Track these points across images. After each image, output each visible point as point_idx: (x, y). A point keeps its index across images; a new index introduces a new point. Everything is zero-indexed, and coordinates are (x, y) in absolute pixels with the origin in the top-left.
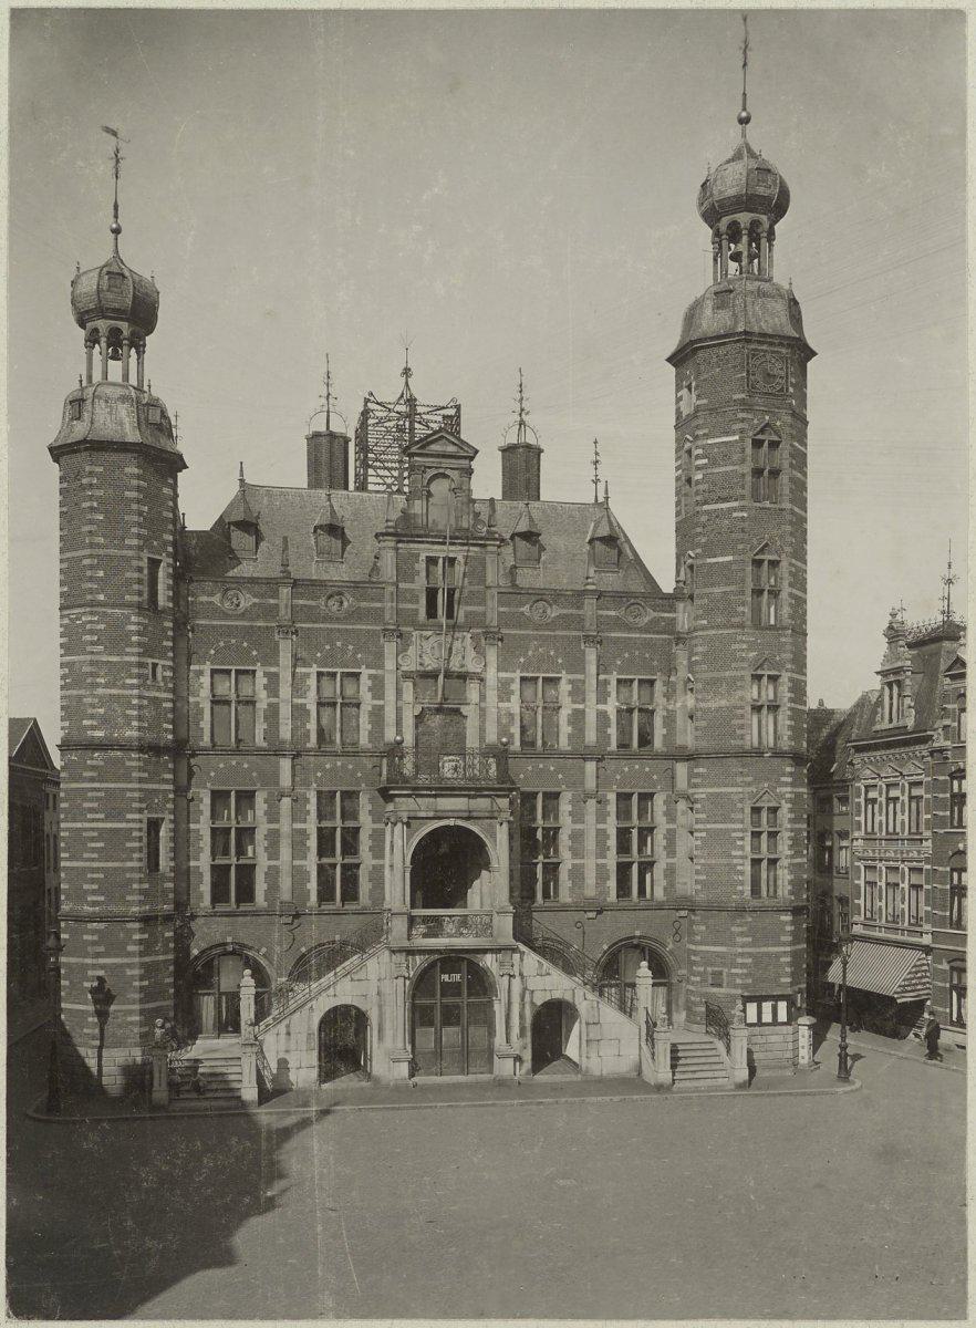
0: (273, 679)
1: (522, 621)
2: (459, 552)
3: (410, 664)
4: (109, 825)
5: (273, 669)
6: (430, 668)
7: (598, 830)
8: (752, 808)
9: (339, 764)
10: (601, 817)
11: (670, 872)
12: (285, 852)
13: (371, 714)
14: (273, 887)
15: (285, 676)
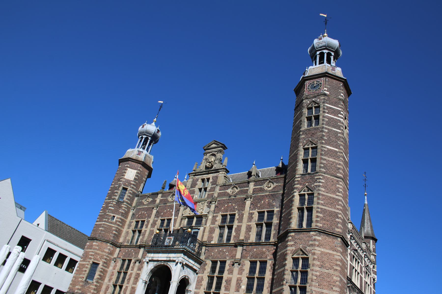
0: (148, 222)
8: (293, 259)
10: (241, 271)
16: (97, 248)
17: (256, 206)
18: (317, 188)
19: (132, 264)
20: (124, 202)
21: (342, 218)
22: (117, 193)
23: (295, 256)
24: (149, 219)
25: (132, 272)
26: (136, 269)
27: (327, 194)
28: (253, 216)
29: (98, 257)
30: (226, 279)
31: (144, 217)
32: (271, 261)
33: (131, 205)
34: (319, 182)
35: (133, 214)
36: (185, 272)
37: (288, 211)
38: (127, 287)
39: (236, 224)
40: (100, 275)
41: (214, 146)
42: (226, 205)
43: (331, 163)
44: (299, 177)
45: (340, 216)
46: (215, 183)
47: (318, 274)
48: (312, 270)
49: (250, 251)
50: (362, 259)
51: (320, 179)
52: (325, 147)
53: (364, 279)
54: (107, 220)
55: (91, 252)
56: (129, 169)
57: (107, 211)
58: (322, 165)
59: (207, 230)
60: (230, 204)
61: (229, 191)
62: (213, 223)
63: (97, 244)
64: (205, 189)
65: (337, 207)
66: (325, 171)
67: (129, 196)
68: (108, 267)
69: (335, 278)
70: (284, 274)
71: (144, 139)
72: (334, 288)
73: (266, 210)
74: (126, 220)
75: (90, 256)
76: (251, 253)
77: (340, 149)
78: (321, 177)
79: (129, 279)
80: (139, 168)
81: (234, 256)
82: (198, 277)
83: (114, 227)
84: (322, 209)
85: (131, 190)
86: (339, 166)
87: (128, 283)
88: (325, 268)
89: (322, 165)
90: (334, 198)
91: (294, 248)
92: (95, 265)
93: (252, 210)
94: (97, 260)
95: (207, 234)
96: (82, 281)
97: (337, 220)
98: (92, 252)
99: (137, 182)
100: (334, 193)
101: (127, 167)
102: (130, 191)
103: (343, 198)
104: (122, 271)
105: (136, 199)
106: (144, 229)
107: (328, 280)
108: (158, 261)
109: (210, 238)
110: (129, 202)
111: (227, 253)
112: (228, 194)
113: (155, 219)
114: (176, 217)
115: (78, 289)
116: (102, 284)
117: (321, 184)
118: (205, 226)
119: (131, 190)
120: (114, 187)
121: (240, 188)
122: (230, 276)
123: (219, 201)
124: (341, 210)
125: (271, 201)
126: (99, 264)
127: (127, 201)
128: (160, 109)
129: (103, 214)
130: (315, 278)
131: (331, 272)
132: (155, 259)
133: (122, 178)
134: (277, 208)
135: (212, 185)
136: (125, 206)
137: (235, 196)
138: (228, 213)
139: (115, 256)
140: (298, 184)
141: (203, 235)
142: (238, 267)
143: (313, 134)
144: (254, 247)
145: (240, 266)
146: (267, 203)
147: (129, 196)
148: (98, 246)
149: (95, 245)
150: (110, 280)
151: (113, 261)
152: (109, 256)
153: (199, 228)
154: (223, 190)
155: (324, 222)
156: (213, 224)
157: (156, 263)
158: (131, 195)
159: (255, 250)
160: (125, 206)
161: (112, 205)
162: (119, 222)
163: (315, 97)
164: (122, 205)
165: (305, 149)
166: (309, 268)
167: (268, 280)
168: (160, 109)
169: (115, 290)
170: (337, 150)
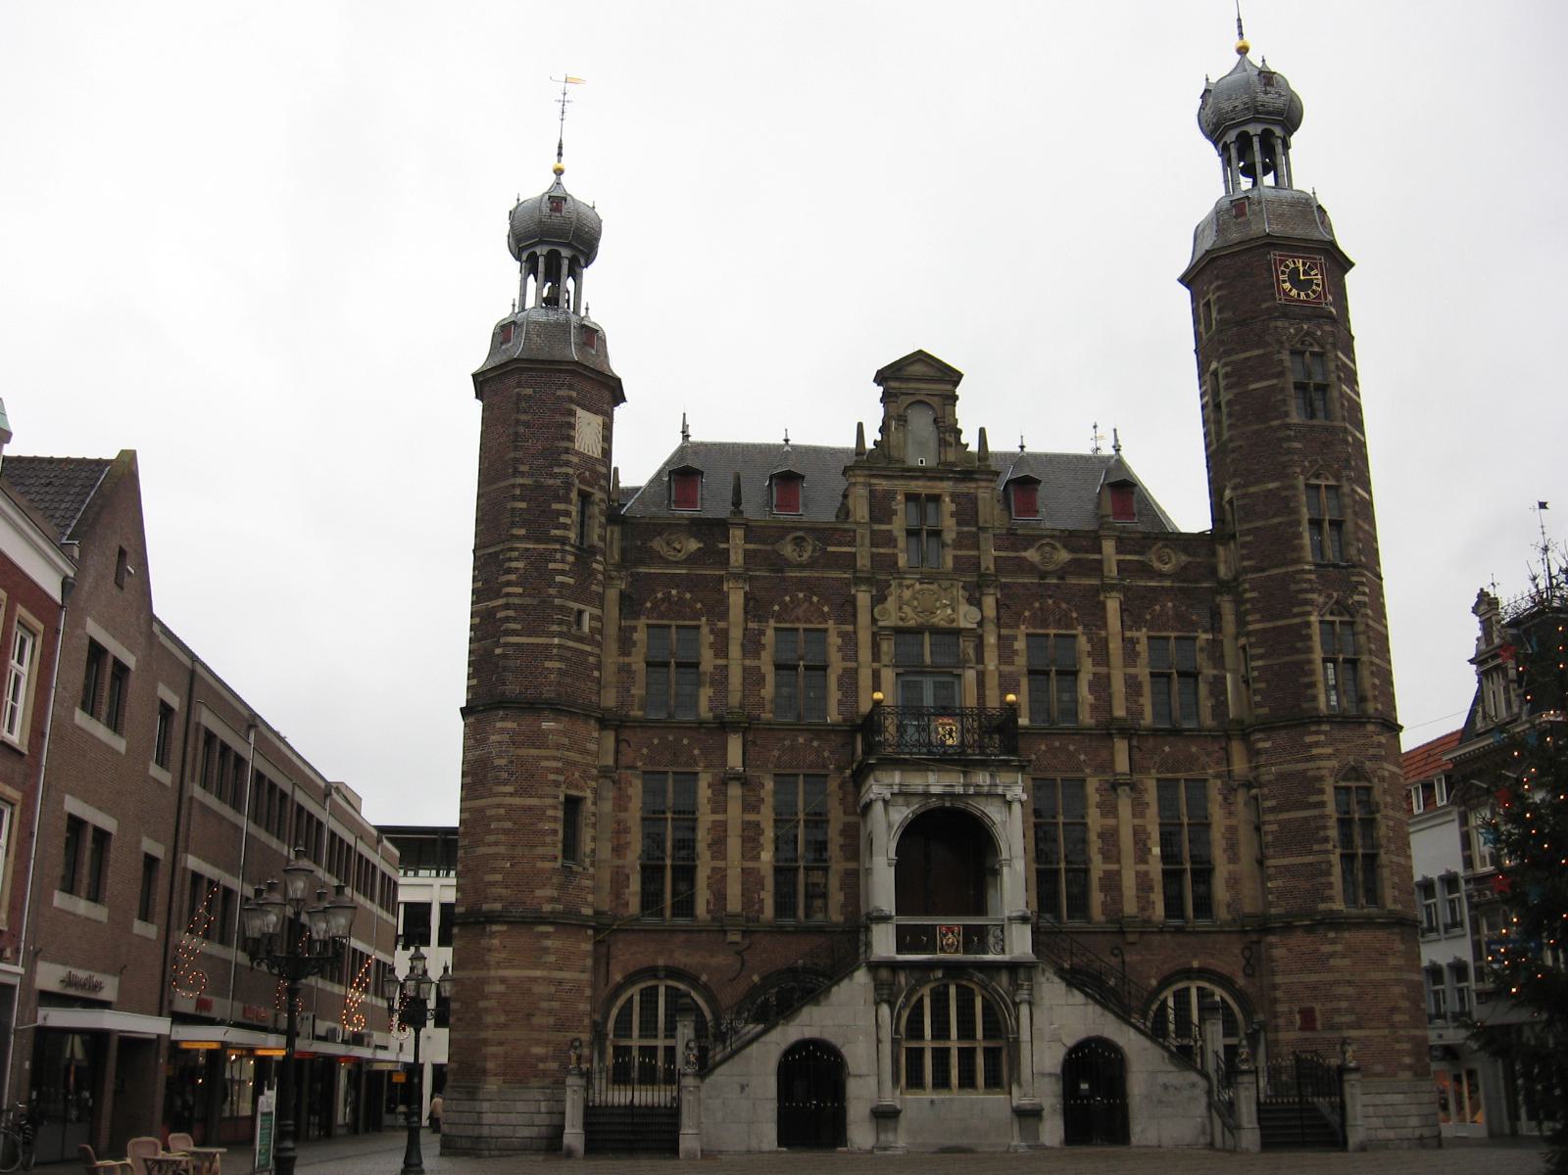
2: (945, 487)
3: (890, 616)
4: (517, 801)
5: (721, 625)
6: (912, 623)
8: (1336, 788)
9: (801, 740)
11: (1233, 882)
12: (734, 845)
13: (840, 679)
14: (720, 897)
15: (736, 634)
16: (566, 741)
18: (1363, 610)
19: (704, 792)
20: (592, 551)
23: (1343, 784)
24: (721, 625)
26: (734, 810)
28: (1138, 648)
29: (577, 774)
30: (1099, 830)
32: (1219, 782)
34: (1364, 594)
35: (624, 597)
39: (1087, 671)
41: (918, 369)
42: (1037, 605)
44: (1310, 572)
48: (1386, 817)
51: (1362, 584)
56: (580, 412)
57: (552, 591)
61: (1031, 555)
63: (561, 727)
64: (936, 533)
70: (1325, 828)
73: (1173, 634)
75: (552, 777)
76: (1157, 758)
81: (1108, 766)
91: (1334, 763)
92: (572, 804)
93: (1131, 629)
94: (577, 787)
98: (555, 759)
101: (571, 400)
106: (708, 661)
108: (927, 795)
111: (1082, 757)
112: (1031, 568)
113: (751, 625)
118: (980, 667)
121: (1072, 550)
122: (1111, 822)
123: (1003, 587)
125: (1183, 608)
129: (528, 601)
132: (912, 789)
133: (567, 451)
134: (1205, 631)
135: (958, 524)
136: (600, 568)
138: (1052, 632)
140: (1312, 591)
142: (1128, 797)
143: (1324, 443)
145: (1133, 795)
148: (565, 733)
150: (618, 850)
153: (956, 671)
154: (1007, 549)
156: (1005, 663)
160: (600, 568)
161: (567, 568)
163: (1308, 318)
164: (595, 565)
166: (1378, 812)
167: (1223, 830)
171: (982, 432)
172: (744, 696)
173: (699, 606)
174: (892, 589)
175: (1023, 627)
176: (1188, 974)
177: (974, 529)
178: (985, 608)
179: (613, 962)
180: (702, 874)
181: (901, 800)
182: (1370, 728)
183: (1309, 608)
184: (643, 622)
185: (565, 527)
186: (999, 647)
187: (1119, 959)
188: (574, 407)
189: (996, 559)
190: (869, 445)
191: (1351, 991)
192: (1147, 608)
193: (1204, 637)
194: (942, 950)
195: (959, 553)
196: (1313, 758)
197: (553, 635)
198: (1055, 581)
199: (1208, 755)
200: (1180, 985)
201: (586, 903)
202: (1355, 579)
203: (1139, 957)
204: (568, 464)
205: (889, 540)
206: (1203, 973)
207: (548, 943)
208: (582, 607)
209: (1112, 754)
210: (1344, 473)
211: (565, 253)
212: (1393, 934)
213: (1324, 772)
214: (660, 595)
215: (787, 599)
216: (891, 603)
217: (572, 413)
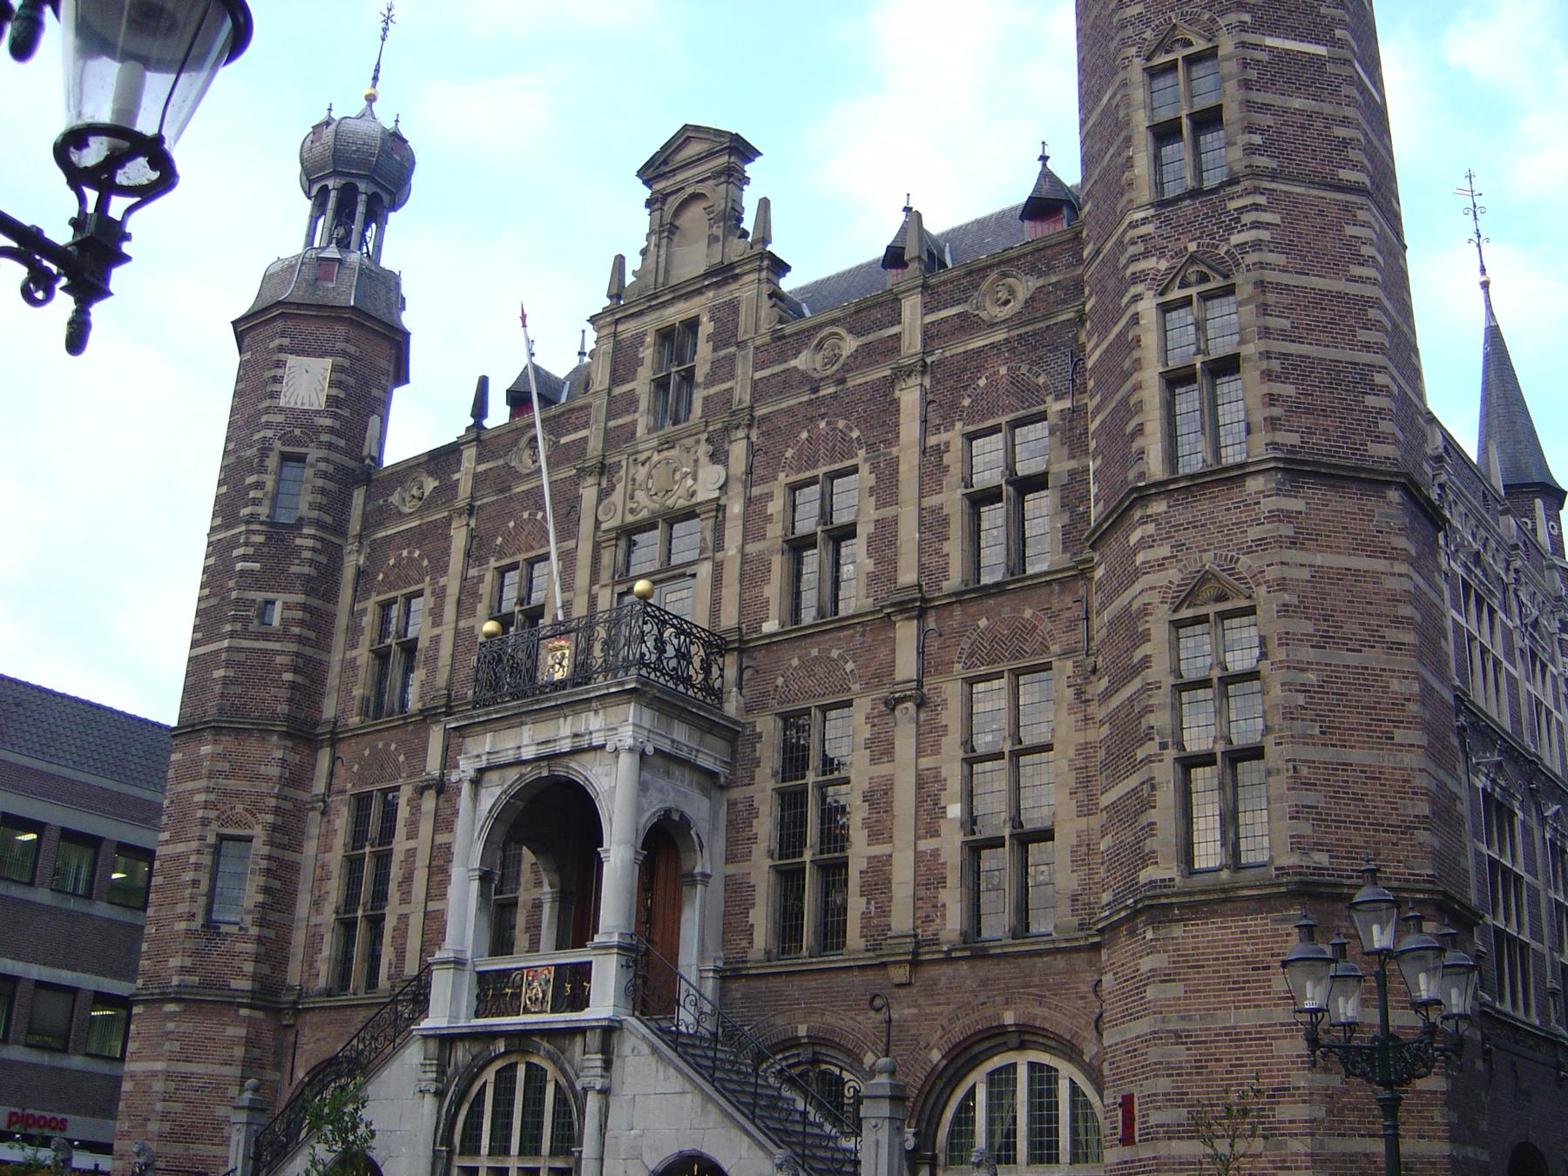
0: (440, 594)
1: (786, 382)
6: (644, 514)
7: (918, 776)
10: (928, 739)
12: (420, 877)
14: (401, 953)
16: (226, 766)
17: (954, 405)
18: (1252, 258)
19: (403, 812)
20: (300, 523)
21: (1395, 389)
22: (259, 485)
23: (1186, 613)
24: (442, 581)
25: (411, 844)
26: (426, 828)
27: (1303, 281)
28: (947, 459)
29: (239, 808)
30: (866, 786)
31: (414, 574)
32: (1069, 663)
33: (340, 529)
34: (1257, 225)
36: (661, 791)
37: (1118, 397)
38: (403, 919)
40: (266, 890)
42: (804, 435)
43: (1301, 120)
44: (1145, 221)
45: (1380, 379)
46: (725, 336)
47: (1312, 677)
49: (961, 634)
50: (1505, 590)
51: (1256, 207)
52: (1255, 46)
53: (1526, 686)
54: (238, 626)
55: (199, 791)
56: (292, 360)
57: (231, 584)
58: (1257, 139)
59: (732, 574)
60: (822, 425)
62: (751, 532)
64: (688, 377)
65: (1363, 336)
66: (1274, 164)
67: (323, 491)
68: (298, 847)
69: (1395, 685)
70: (1148, 710)
71: (333, 194)
72: (1400, 735)
74: (330, 607)
77: (1333, 42)
78: (1262, 200)
79: (408, 879)
80: (339, 346)
82: (732, 804)
83: (282, 651)
84: (1285, 356)
85: (327, 460)
86: (1342, 132)
87: (406, 898)
88: (1344, 643)
89: (1257, 139)
90: (1340, 296)
91: (1173, 574)
94: (238, 824)
95: (731, 591)
96: (189, 933)
97: (1371, 401)
98: (208, 790)
99: (346, 413)
100: (1336, 267)
101: (281, 349)
102: (322, 466)
103: (1384, 288)
104: (368, 849)
105: (358, 496)
107: (1367, 699)
108: (520, 763)
109: (751, 607)
110: (329, 520)
111: (850, 666)
113: (473, 572)
114: (571, 544)
115: (183, 970)
116: (290, 928)
117: (1265, 235)
118: (719, 556)
119: (327, 460)
120: (240, 460)
121: (859, 334)
122: (884, 769)
123: (766, 418)
124: (1381, 349)
126: (249, 839)
127: (315, 514)
128: (385, 30)
130: (1301, 699)
131: (1374, 657)
133: (267, 410)
134: (1059, 397)
135: (715, 350)
136: (310, 543)
137: (842, 381)
139: (320, 787)
140: (1145, 255)
141: (716, 603)
144: (973, 609)
146: (1004, 383)
147: (323, 491)
148: (223, 757)
149: (214, 757)
150: (317, 904)
151: (315, 816)
152: (288, 792)
153: (689, 571)
154: (772, 363)
155: (1306, 421)
157: (512, 775)
158: (330, 485)
159: (983, 623)
160: (310, 543)
161: (250, 551)
162: (302, 623)
164: (298, 541)
165: (1153, 73)
167: (1071, 753)
168: (385, 30)
169: (349, 940)
170: (1321, 50)
171: (764, 205)
172: (453, 670)
173: (426, 563)
174: (623, 473)
175: (781, 476)
176: (996, 1037)
177: (733, 349)
178: (731, 460)
179: (298, 1051)
180: (390, 923)
181: (493, 776)
182: (1254, 485)
183: (1139, 288)
184: (371, 604)
185: (256, 502)
186: (746, 518)
187: (881, 1016)
188: (282, 356)
189: (755, 383)
190: (629, 279)
191: (1180, 1053)
192: (965, 388)
193: (1054, 407)
194: (527, 1011)
195: (712, 391)
196: (1136, 574)
197: (222, 637)
198: (832, 390)
199: (1053, 617)
200: (997, 1062)
201: (240, 973)
202: (1232, 205)
203: (915, 1011)
204: (268, 425)
205: (631, 402)
206: (1025, 1036)
207: (171, 1026)
208: (270, 596)
209: (893, 651)
210: (1222, 22)
211: (331, 183)
212: (1285, 920)
213: (1154, 597)
214: (392, 562)
215: (512, 524)
216: (618, 496)
217: (280, 364)
